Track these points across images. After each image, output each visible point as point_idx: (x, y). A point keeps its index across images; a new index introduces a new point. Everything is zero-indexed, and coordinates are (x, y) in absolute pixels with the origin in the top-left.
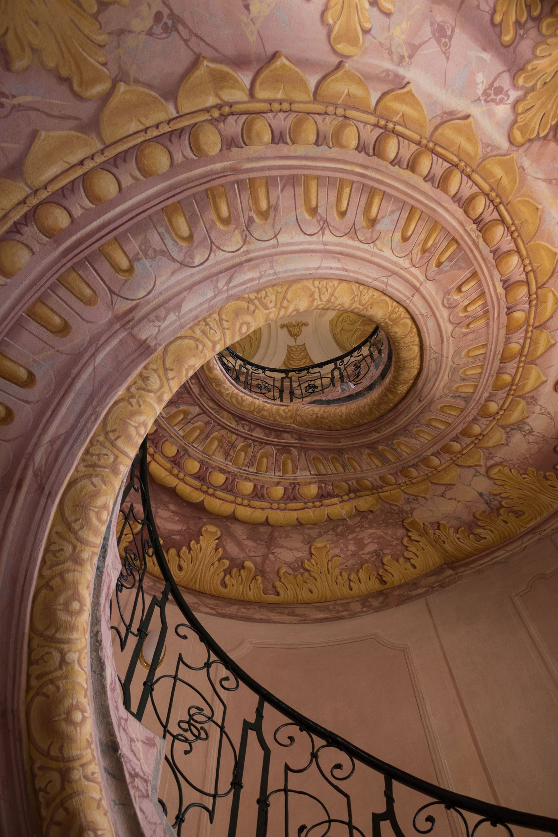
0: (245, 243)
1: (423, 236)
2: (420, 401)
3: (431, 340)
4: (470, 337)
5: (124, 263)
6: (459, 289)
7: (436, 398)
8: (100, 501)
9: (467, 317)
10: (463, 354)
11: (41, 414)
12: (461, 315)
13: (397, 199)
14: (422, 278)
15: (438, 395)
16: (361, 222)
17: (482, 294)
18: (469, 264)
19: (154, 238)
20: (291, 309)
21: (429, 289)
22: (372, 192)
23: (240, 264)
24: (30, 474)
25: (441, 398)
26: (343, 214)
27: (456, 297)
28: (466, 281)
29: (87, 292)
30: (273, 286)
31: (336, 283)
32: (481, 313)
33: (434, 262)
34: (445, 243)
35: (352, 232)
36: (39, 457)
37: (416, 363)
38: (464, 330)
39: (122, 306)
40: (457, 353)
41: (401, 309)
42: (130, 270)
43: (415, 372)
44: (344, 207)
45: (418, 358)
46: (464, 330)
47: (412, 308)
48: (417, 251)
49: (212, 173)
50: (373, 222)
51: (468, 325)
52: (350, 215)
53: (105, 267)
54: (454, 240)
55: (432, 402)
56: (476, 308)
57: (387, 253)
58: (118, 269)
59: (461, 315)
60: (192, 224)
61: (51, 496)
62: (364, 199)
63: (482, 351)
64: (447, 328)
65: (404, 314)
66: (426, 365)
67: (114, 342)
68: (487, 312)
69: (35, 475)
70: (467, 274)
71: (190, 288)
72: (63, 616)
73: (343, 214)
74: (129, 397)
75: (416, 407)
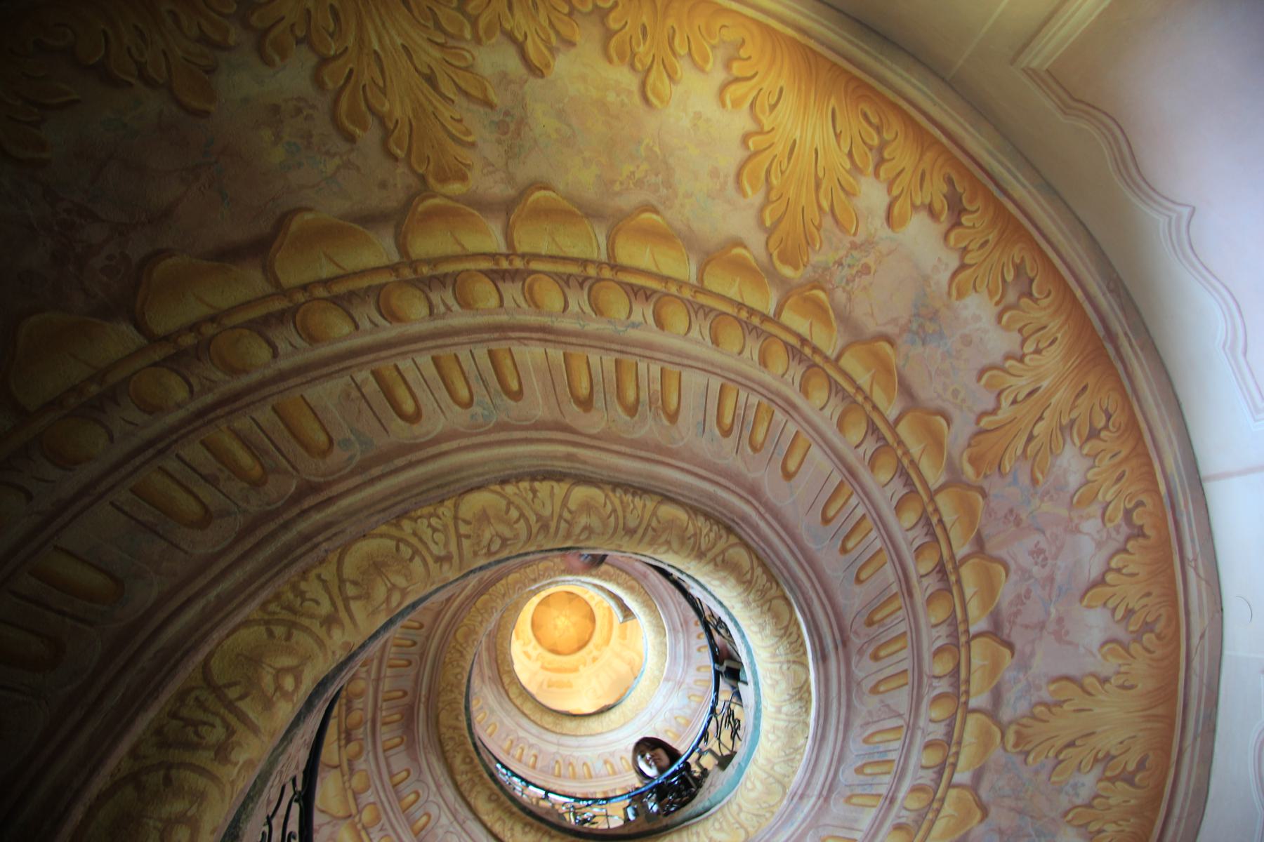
0: (655, 728)
1: (577, 770)
2: (489, 678)
3: (524, 722)
4: (503, 736)
5: (692, 698)
6: (536, 757)
7: (484, 687)
8: (652, 637)
9: (517, 745)
10: (498, 725)
11: (689, 644)
12: (521, 745)
13: (601, 777)
14: (560, 751)
15: (484, 687)
16: (611, 759)
17: (520, 760)
18: (542, 771)
19: (688, 712)
20: (618, 713)
21: (553, 749)
22: (615, 773)
23: (650, 721)
24: (680, 629)
25: (481, 688)
26: (621, 758)
27: (534, 752)
28: (535, 762)
29: (699, 683)
30: (632, 719)
31: (604, 730)
32: (511, 752)
33: (561, 761)
34: (562, 772)
35: (612, 754)
36: (681, 635)
37: (518, 702)
38: (511, 737)
39: (684, 686)
40: (502, 723)
41: (558, 731)
42: (689, 698)
43: (512, 696)
44: (623, 761)
45: (520, 706)
46: (511, 737)
47: (554, 735)
48: (575, 762)
49: (684, 742)
50: (606, 762)
51: (512, 742)
52: (618, 759)
53: (699, 693)
54: (559, 776)
55: (483, 681)
56: (517, 753)
57: (589, 754)
58: (694, 695)
59: (521, 745)
60: (679, 724)
61: (670, 630)
62: (616, 768)
63: (489, 731)
64: (522, 734)
65: (554, 729)
66: (511, 705)
67: (679, 676)
68: (509, 754)
69: (678, 631)
70: (539, 765)
71: (664, 704)
72: (644, 609)
73: (621, 758)
74: (663, 665)
75: (487, 672)
